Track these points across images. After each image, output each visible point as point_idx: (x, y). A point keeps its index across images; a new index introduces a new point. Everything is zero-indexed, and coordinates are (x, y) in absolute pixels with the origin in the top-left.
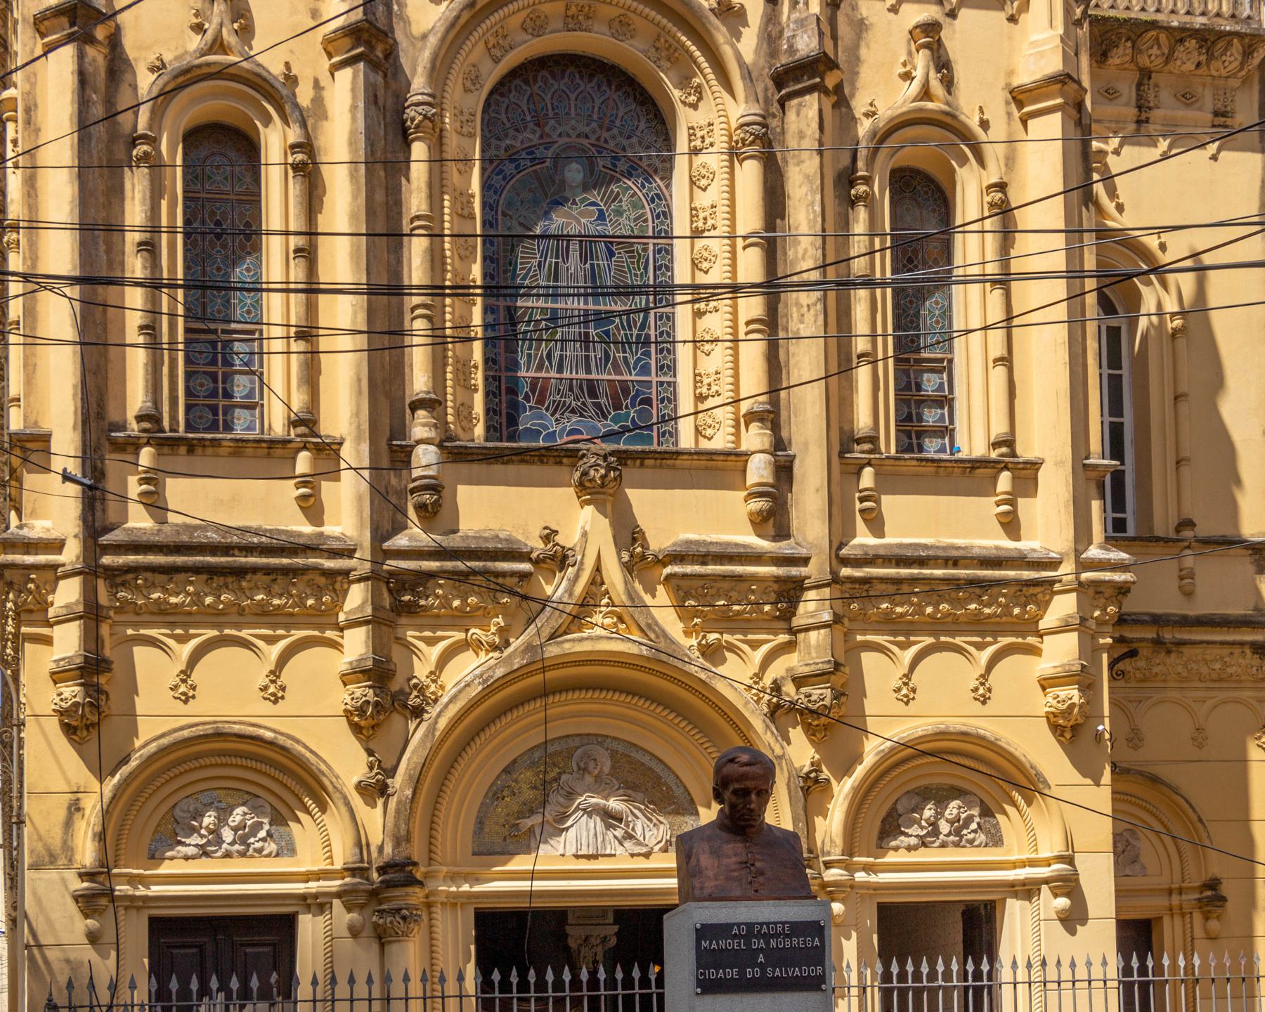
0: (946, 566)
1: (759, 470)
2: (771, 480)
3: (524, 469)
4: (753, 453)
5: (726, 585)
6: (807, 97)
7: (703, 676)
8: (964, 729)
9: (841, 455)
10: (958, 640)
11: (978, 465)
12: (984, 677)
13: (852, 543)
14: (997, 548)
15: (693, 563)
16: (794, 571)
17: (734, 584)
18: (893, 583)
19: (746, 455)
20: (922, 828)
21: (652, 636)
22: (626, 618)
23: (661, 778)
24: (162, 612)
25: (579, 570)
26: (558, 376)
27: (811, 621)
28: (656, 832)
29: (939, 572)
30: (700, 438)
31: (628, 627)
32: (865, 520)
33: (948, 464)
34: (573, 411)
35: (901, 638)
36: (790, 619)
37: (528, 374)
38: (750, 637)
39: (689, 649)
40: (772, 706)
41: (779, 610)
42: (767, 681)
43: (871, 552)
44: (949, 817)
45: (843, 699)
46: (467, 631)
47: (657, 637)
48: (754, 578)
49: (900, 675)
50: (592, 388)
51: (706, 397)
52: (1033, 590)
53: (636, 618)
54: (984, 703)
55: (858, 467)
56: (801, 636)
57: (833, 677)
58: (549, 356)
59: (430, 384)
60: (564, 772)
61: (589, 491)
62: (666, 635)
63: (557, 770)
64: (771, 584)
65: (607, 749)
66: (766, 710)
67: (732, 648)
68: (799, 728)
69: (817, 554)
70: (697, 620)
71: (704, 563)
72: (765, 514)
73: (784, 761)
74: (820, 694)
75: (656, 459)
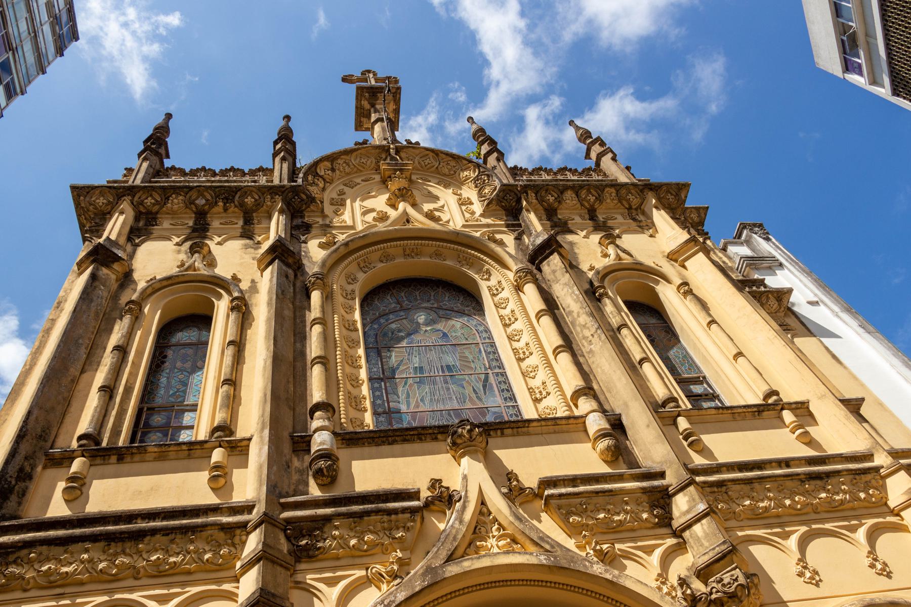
0: (780, 467)
1: (595, 423)
4: (587, 415)
5: (600, 500)
6: (551, 257)
11: (762, 408)
15: (565, 486)
16: (656, 483)
17: (607, 497)
18: (745, 484)
19: (582, 417)
21: (548, 547)
22: (519, 537)
24: (51, 585)
32: (696, 451)
33: (740, 410)
36: (670, 525)
38: (640, 544)
40: (689, 599)
41: (656, 516)
42: (673, 580)
46: (367, 569)
48: (622, 491)
51: (541, 400)
53: (527, 533)
56: (686, 534)
59: (324, 397)
67: (627, 556)
69: (668, 468)
71: (574, 486)
72: (613, 448)
74: (731, 576)
75: (512, 428)
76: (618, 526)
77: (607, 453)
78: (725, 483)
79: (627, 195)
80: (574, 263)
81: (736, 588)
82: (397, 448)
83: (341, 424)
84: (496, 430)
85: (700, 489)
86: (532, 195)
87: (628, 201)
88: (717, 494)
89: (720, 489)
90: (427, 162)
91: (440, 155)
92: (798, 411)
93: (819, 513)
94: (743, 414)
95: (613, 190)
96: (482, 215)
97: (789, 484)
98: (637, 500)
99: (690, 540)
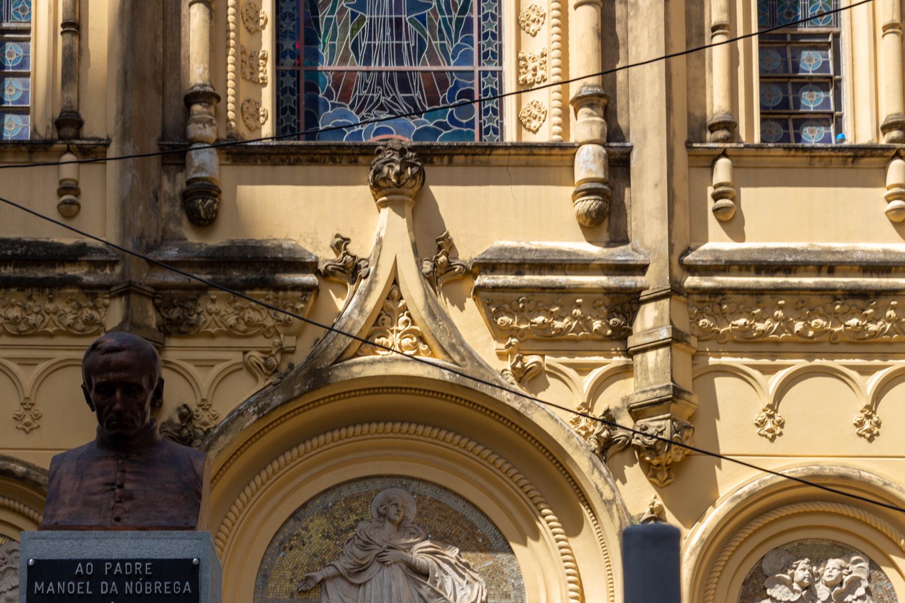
2: (600, 175)
3: (314, 169)
5: (546, 297)
7: (516, 405)
8: (843, 471)
9: (688, 145)
10: (836, 363)
11: (861, 153)
12: (870, 410)
13: (702, 248)
14: (885, 252)
16: (628, 281)
17: (555, 295)
18: (752, 294)
20: (794, 592)
22: (428, 338)
23: (477, 528)
25: (371, 282)
26: (365, 68)
27: (648, 339)
28: (469, 591)
29: (809, 281)
30: (524, 131)
31: (430, 348)
32: (721, 222)
33: (823, 153)
34: (382, 108)
35: (765, 362)
36: (624, 339)
37: (331, 68)
39: (501, 374)
41: (611, 328)
42: (598, 412)
43: (724, 258)
44: (829, 579)
45: (687, 433)
47: (463, 359)
48: (578, 290)
49: (763, 405)
50: (404, 81)
54: (871, 440)
55: (712, 159)
56: (638, 358)
57: (673, 406)
58: (355, 47)
60: (362, 519)
61: (384, 192)
62: (472, 356)
63: (353, 517)
64: (601, 296)
65: (413, 494)
66: (594, 445)
67: (555, 373)
68: (637, 466)
69: (655, 261)
70: (514, 341)
72: (594, 215)
73: (614, 507)
75: (466, 155)
76: (557, 334)
77: (585, 219)
78: (724, 292)
82: (300, 170)
83: (228, 120)
84: (442, 155)
88: (706, 304)
89: (713, 299)
93: (837, 343)
97: (816, 300)
98: (595, 302)
99: (638, 368)
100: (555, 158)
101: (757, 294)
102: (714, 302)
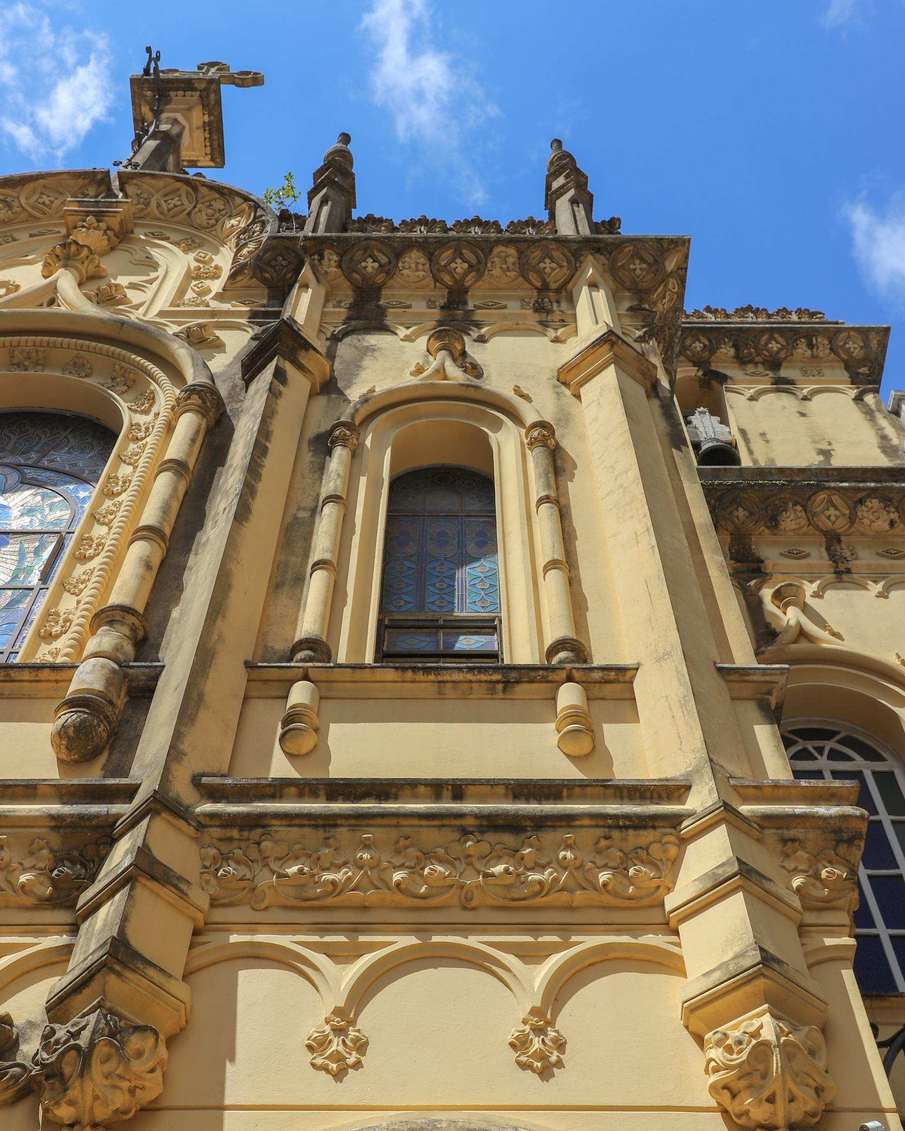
11: (514, 675)
18: (316, 826)
52: (634, 838)
72: (71, 731)
78: (266, 822)
79: (542, 260)
80: (340, 385)
81: (63, 1054)
85: (191, 831)
86: (331, 257)
87: (541, 273)
88: (236, 844)
89: (246, 834)
90: (176, 201)
91: (201, 189)
92: (608, 686)
94: (465, 685)
95: (512, 251)
96: (219, 297)
97: (430, 835)
100: (44, 685)
101: (324, 826)
102: (248, 839)
